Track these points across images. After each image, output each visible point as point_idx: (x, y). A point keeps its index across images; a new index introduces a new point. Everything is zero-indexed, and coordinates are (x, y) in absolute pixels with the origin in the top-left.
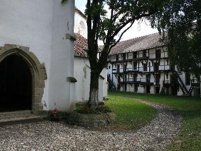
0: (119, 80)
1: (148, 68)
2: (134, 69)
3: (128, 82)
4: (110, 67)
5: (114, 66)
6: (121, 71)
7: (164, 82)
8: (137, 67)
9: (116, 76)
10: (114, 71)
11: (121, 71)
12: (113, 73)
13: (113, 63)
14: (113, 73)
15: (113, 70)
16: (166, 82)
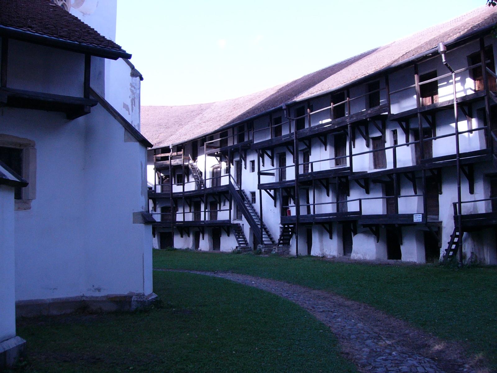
0: (284, 212)
1: (389, 154)
2: (337, 164)
3: (315, 215)
4: (253, 162)
5: (267, 160)
6: (290, 175)
7: (457, 206)
8: (348, 153)
9: (274, 198)
10: (265, 180)
11: (290, 175)
12: (261, 187)
13: (262, 150)
14: (261, 187)
15: (260, 173)
16: (466, 209)
